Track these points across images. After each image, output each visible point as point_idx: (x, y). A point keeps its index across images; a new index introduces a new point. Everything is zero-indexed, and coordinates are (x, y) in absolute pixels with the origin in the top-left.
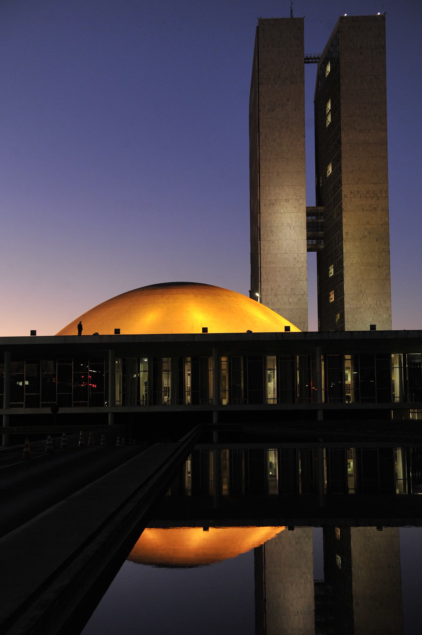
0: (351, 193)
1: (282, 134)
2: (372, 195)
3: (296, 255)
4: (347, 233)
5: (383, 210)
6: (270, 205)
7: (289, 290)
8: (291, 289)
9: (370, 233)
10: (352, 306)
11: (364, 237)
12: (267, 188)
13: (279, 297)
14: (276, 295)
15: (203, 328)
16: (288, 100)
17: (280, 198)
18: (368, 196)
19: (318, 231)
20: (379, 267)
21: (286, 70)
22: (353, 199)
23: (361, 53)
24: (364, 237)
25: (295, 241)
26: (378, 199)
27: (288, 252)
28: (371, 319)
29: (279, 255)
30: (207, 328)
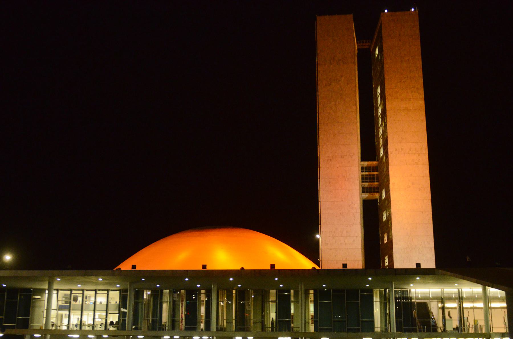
0: (396, 150)
1: (337, 103)
3: (351, 203)
6: (328, 160)
8: (347, 232)
9: (413, 184)
15: (271, 265)
16: (342, 76)
17: (336, 154)
19: (374, 182)
20: (422, 212)
21: (339, 53)
23: (400, 40)
26: (419, 155)
27: (344, 200)
29: (336, 203)
30: (274, 265)
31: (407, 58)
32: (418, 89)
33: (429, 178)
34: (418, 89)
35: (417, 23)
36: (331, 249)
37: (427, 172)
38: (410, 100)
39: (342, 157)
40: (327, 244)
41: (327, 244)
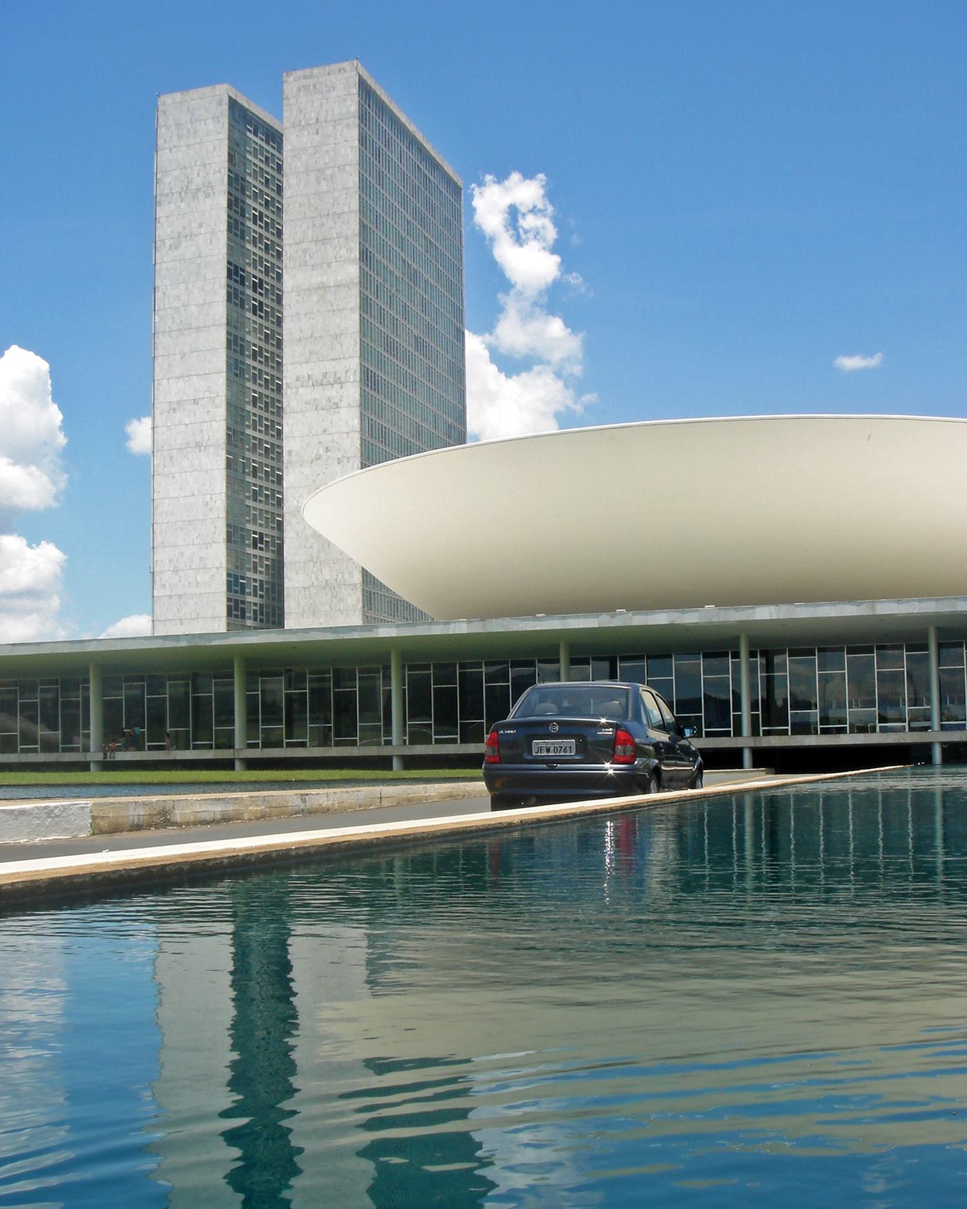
0: (298, 379)
2: (332, 381)
4: (290, 452)
5: (349, 406)
7: (196, 560)
9: (327, 450)
10: (297, 585)
11: (318, 457)
12: (165, 382)
13: (181, 573)
14: (176, 571)
16: (200, 225)
18: (325, 382)
22: (301, 390)
23: (317, 133)
24: (318, 457)
25: (206, 471)
28: (327, 608)
31: (329, 172)
32: (347, 238)
33: (358, 436)
34: (347, 238)
35: (355, 90)
36: (170, 596)
37: (357, 422)
38: (329, 265)
39: (195, 402)
40: (164, 586)
41: (164, 586)
